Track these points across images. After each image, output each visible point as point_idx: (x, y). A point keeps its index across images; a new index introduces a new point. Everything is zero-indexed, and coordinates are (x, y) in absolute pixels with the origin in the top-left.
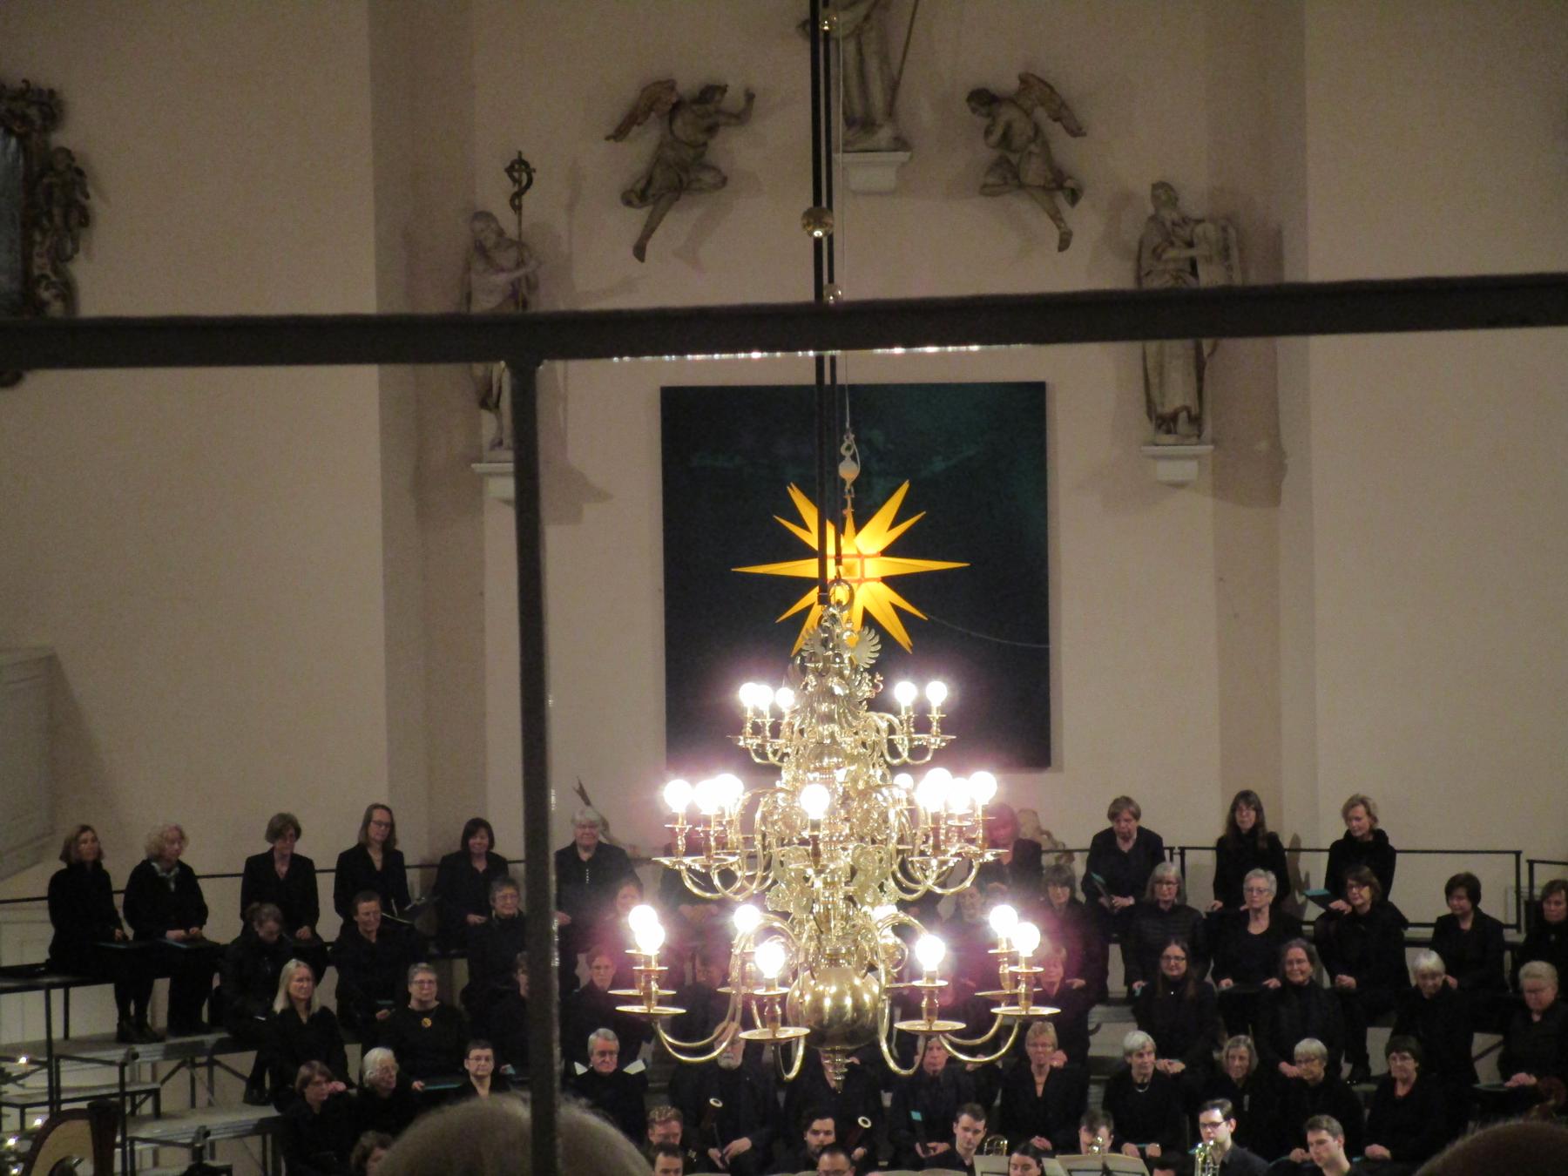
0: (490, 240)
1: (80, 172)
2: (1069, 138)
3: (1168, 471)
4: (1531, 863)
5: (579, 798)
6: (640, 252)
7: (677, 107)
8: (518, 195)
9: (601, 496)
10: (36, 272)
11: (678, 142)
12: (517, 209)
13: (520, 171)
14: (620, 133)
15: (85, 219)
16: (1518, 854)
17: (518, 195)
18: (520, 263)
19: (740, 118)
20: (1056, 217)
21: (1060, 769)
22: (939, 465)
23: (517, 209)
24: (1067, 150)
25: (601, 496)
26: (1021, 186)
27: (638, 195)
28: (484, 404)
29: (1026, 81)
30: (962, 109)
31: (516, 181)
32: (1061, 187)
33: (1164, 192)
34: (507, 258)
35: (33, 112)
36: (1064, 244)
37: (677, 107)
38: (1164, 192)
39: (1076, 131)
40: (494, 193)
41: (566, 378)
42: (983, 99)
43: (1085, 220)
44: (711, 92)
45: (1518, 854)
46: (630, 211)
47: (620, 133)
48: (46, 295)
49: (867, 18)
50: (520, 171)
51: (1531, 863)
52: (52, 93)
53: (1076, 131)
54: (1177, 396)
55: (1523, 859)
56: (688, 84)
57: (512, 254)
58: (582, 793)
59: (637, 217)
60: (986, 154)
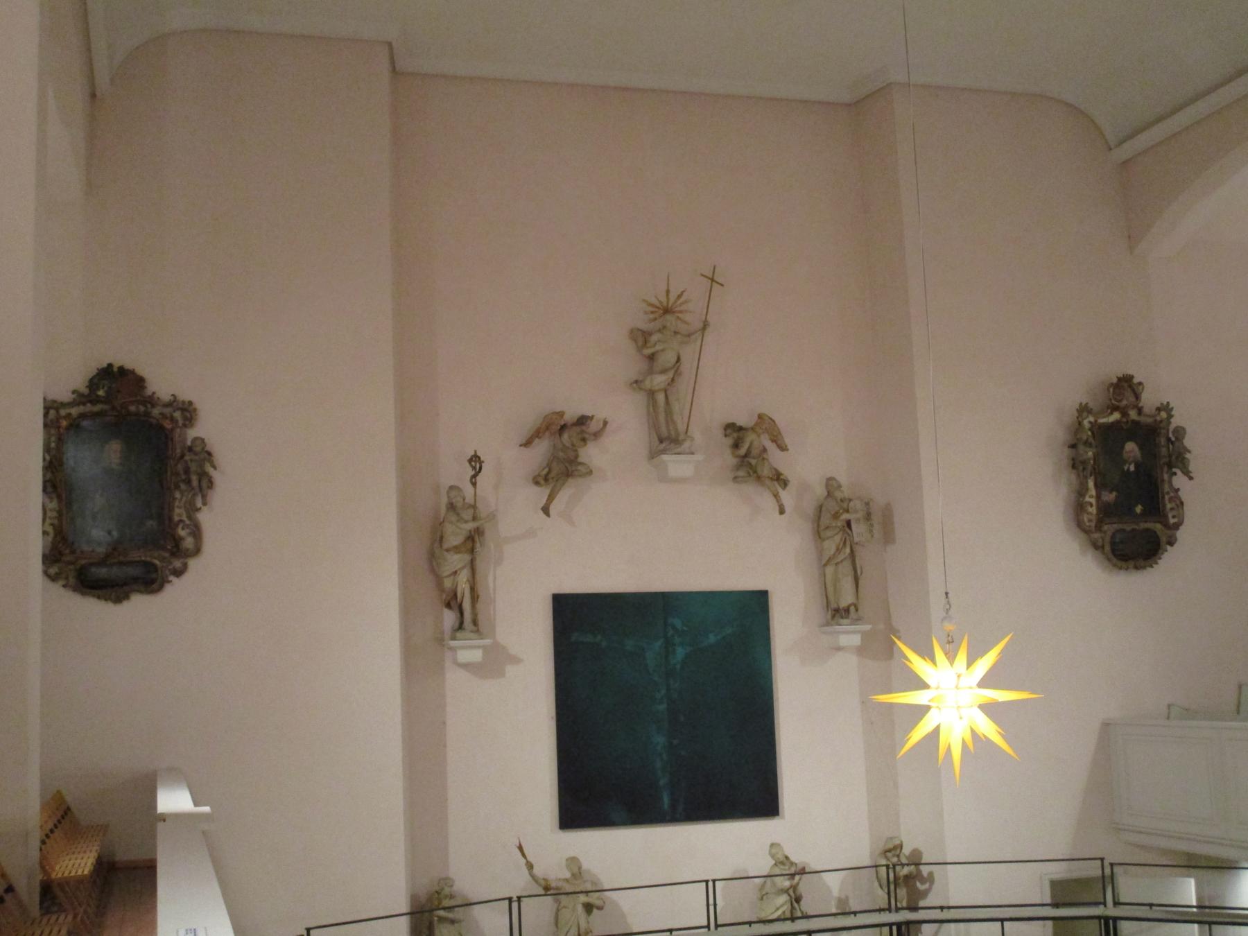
0: (459, 505)
1: (209, 454)
2: (778, 451)
3: (844, 640)
4: (1112, 865)
5: (518, 851)
6: (546, 510)
7: (563, 428)
8: (474, 476)
9: (515, 660)
10: (176, 518)
11: (562, 450)
12: (474, 484)
13: (476, 461)
14: (527, 443)
15: (211, 484)
16: (1102, 860)
17: (474, 476)
18: (474, 519)
19: (597, 435)
20: (776, 496)
21: (783, 818)
22: (712, 639)
23: (474, 484)
24: (777, 459)
25: (515, 660)
26: (759, 478)
27: (540, 479)
28: (448, 606)
29: (760, 417)
30: (719, 433)
31: (474, 468)
32: (780, 479)
33: (831, 485)
34: (467, 515)
35: (177, 415)
36: (782, 512)
37: (563, 428)
38: (831, 485)
39: (783, 448)
40: (455, 472)
41: (494, 590)
42: (735, 432)
43: (787, 497)
44: (582, 421)
45: (1102, 860)
46: (536, 489)
47: (527, 443)
48: (182, 532)
49: (673, 380)
50: (476, 461)
51: (1112, 865)
52: (190, 403)
53: (783, 448)
54: (847, 599)
55: (1106, 863)
56: (571, 414)
57: (471, 511)
58: (520, 848)
59: (542, 493)
60: (731, 460)
